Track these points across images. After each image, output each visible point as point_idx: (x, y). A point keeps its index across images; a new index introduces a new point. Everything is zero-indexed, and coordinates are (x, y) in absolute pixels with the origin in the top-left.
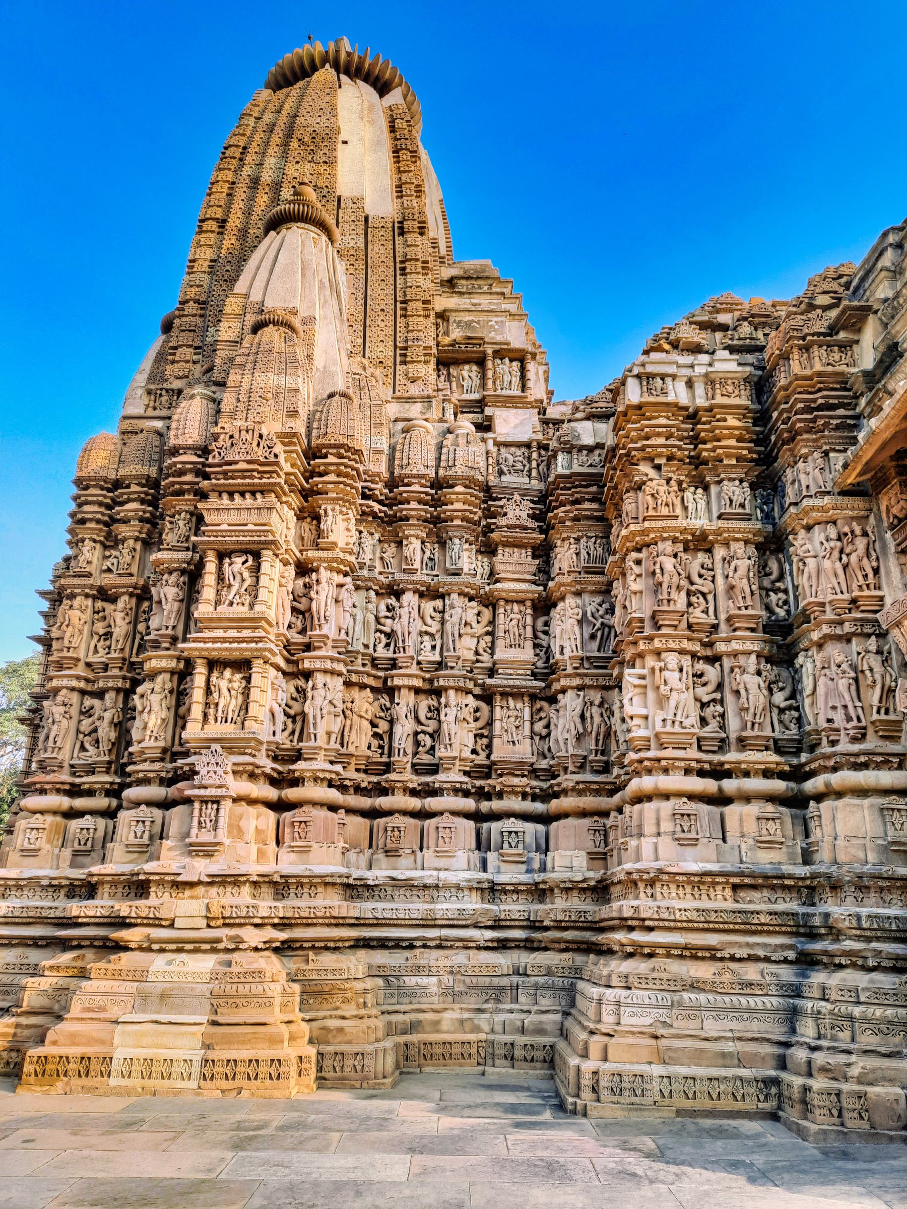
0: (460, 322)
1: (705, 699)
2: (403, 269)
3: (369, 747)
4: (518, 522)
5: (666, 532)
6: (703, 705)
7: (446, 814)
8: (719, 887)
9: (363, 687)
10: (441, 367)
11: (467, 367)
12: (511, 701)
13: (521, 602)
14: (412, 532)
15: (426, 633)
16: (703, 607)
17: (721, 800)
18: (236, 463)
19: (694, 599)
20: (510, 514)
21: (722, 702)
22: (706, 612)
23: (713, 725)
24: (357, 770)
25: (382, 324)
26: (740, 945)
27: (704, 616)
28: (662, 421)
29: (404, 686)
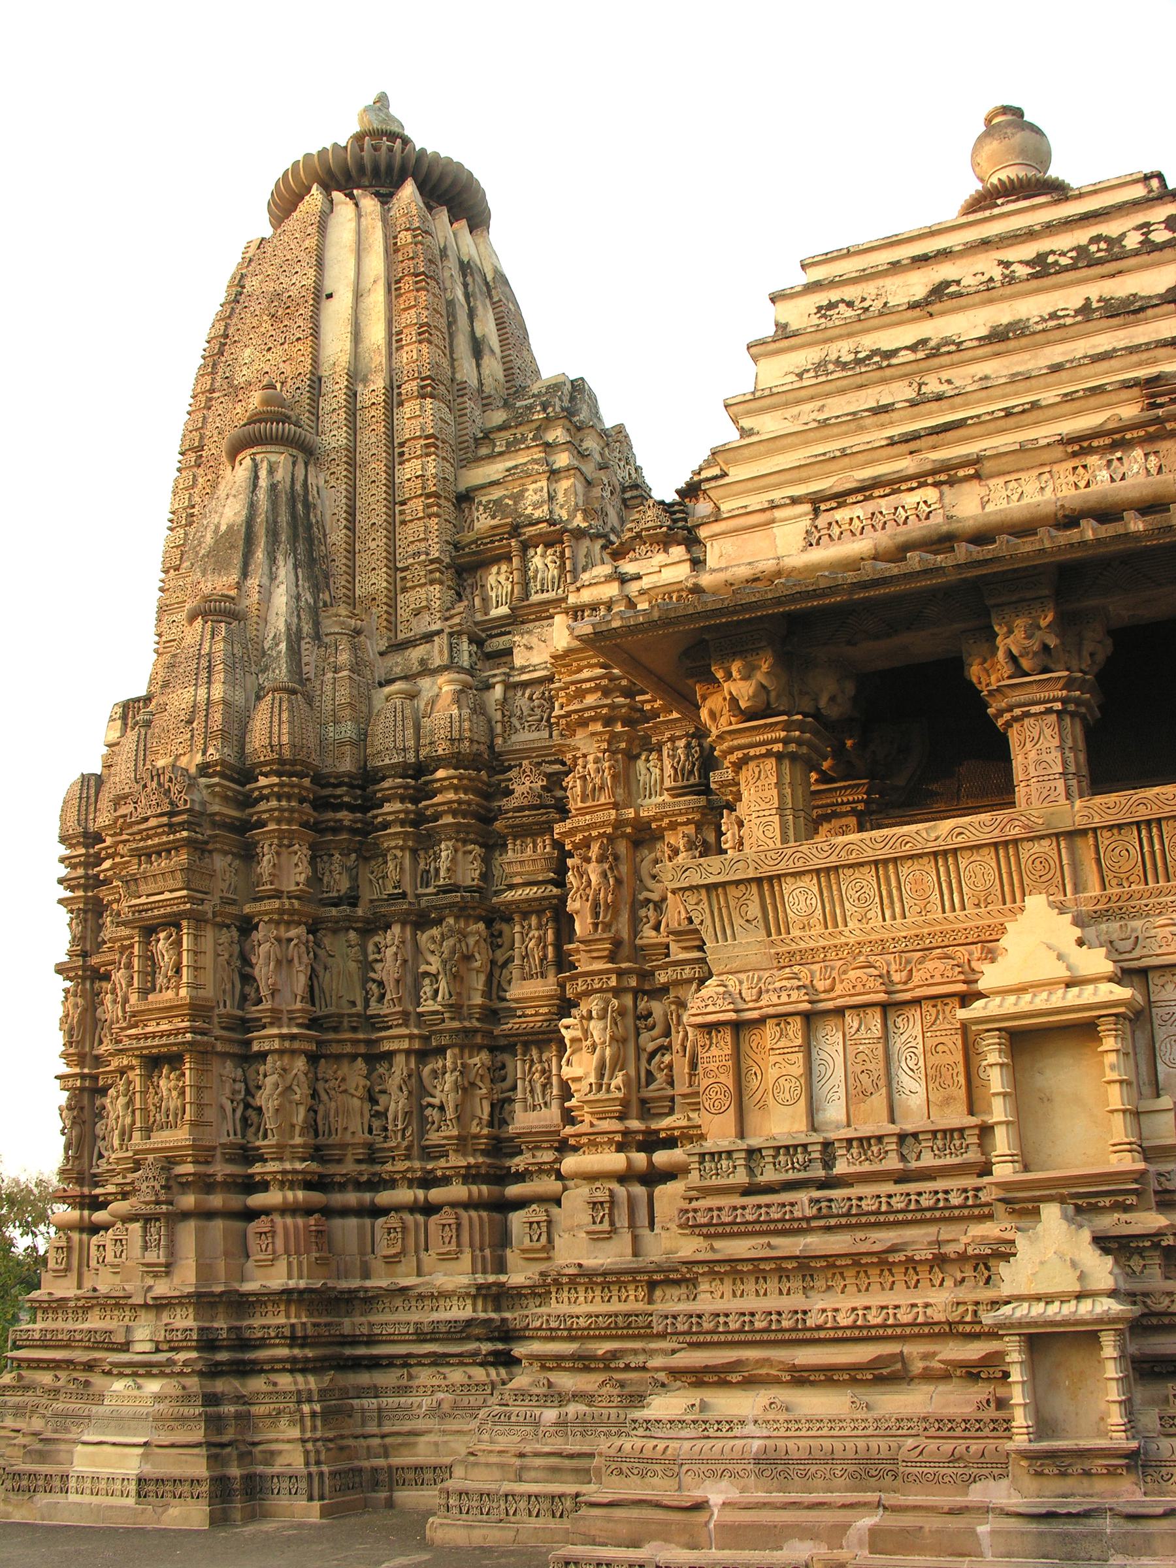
0: (489, 502)
1: (651, 1047)
2: (402, 454)
3: (370, 1131)
4: (526, 803)
5: (595, 828)
6: (652, 1055)
7: (446, 1208)
8: (631, 1287)
9: (353, 1057)
10: (465, 575)
11: (494, 569)
12: (535, 1053)
13: (539, 913)
14: (393, 844)
15: (427, 974)
16: (652, 922)
17: (654, 1177)
18: (146, 819)
19: (642, 912)
20: (519, 789)
21: (668, 1048)
22: (657, 928)
23: (660, 1077)
24: (359, 1161)
25: (373, 545)
26: (635, 1352)
27: (654, 933)
28: (586, 674)
29: (399, 1051)
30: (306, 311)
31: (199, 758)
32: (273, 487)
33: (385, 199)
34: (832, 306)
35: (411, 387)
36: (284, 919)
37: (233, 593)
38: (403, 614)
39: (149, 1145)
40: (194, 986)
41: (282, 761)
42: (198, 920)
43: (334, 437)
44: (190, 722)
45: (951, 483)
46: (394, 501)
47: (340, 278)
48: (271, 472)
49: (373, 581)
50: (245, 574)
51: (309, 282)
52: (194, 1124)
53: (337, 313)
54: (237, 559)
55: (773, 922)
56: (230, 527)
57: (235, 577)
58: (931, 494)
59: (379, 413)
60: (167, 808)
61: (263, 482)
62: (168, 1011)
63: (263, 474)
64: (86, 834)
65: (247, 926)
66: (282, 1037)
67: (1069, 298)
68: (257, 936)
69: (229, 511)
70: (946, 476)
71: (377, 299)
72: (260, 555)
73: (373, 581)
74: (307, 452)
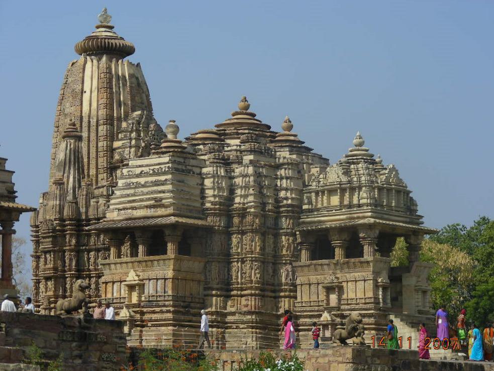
30: (79, 97)
31: (54, 217)
32: (71, 149)
33: (99, 60)
34: (129, 171)
35: (101, 122)
36: (71, 251)
37: (62, 177)
38: (99, 179)
39: (46, 295)
40: (54, 264)
41: (70, 218)
42: (54, 251)
43: (85, 134)
44: (53, 209)
45: (133, 209)
46: (97, 152)
47: (87, 87)
48: (70, 145)
49: (93, 172)
50: (64, 173)
51: (80, 88)
52: (54, 291)
53: (86, 97)
54: (62, 170)
55: (110, 270)
56: (62, 160)
57: (62, 174)
58: (130, 210)
59: (95, 128)
60: (47, 228)
61: (68, 148)
62: (49, 269)
63: (69, 145)
64: (35, 225)
65: (64, 251)
66: (71, 274)
67: (154, 179)
68: (66, 254)
69: (61, 156)
70: (133, 208)
71: (95, 94)
72: (67, 168)
73: (93, 172)
74: (80, 138)
